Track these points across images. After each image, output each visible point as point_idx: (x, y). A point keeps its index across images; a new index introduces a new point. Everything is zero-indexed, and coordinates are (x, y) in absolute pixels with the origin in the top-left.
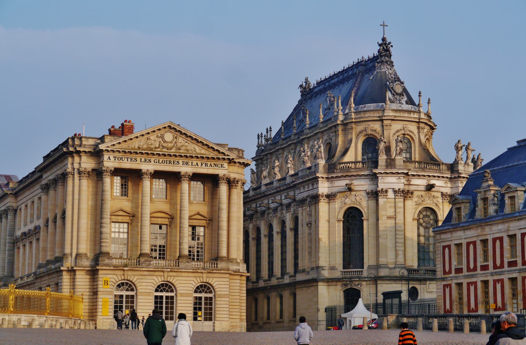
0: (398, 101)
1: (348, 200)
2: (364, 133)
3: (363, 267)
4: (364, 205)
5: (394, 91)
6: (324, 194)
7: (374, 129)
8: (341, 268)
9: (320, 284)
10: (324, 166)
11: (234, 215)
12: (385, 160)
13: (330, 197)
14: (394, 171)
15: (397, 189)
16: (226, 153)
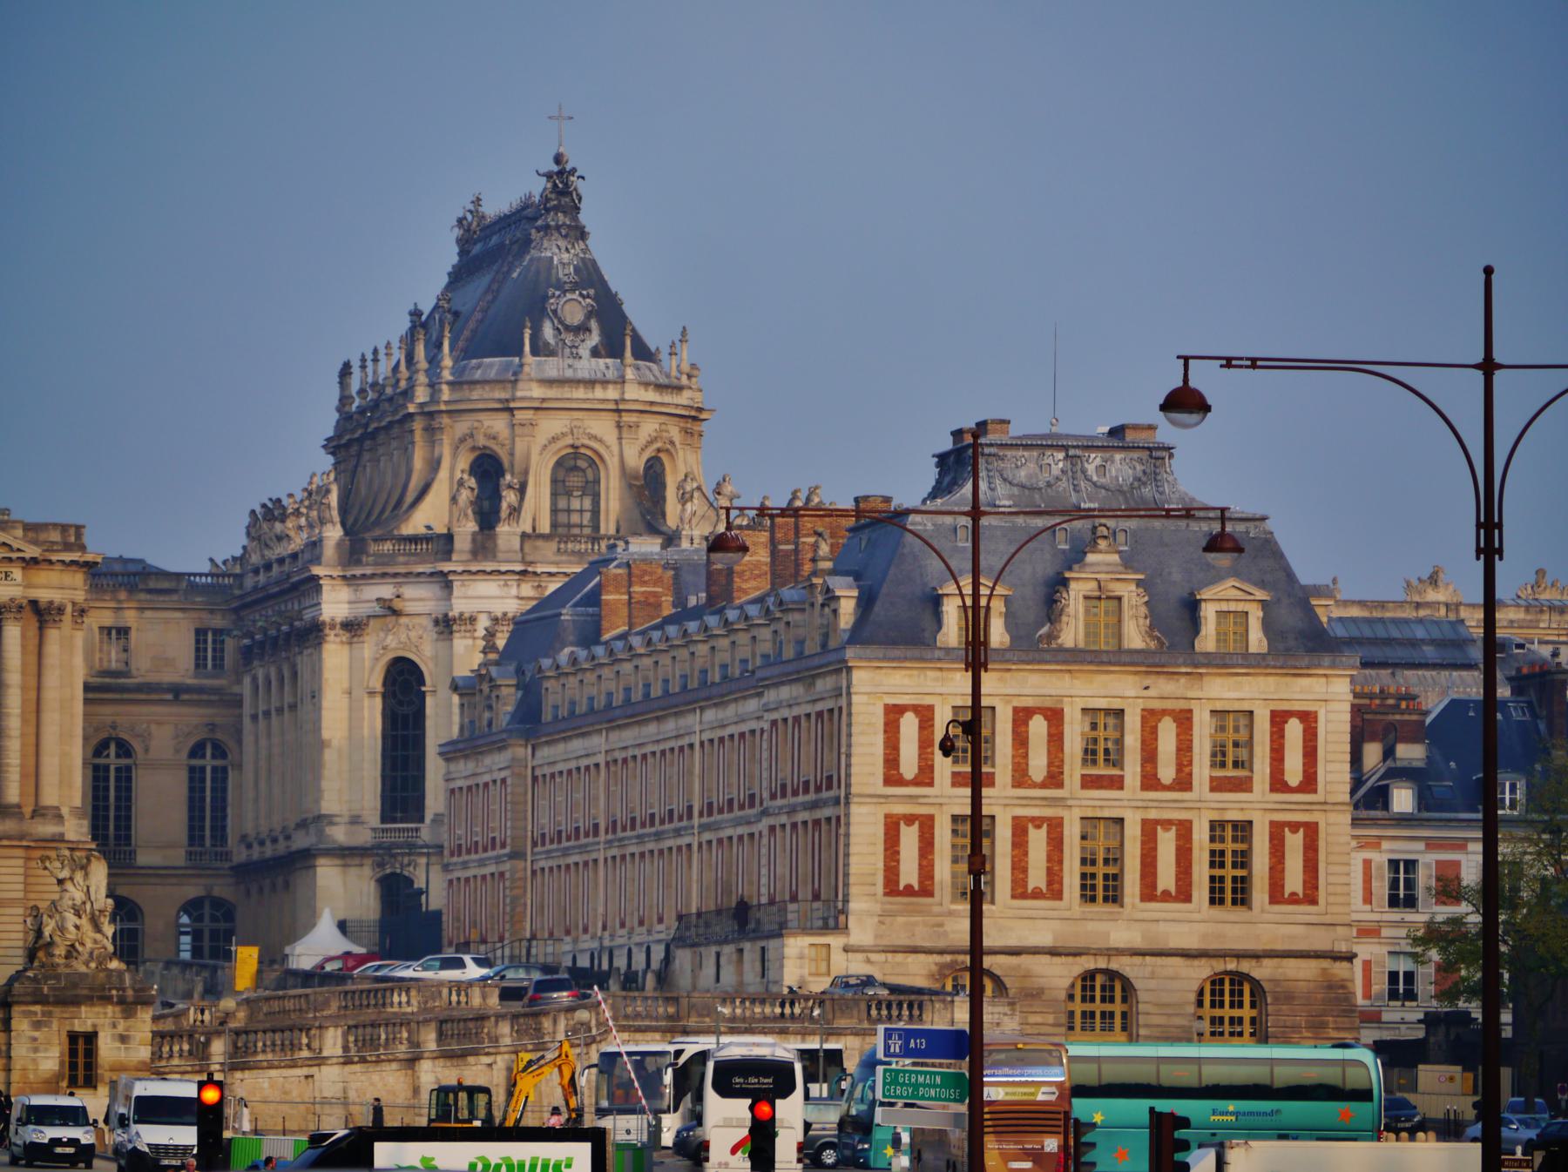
0: (567, 351)
1: (390, 637)
2: (470, 443)
3: (421, 820)
4: (425, 653)
5: (561, 322)
6: (338, 620)
7: (492, 431)
8: (374, 820)
9: (321, 861)
10: (339, 544)
11: (51, 695)
12: (469, 538)
13: (353, 627)
14: (489, 567)
15: (499, 615)
16: (15, 546)
